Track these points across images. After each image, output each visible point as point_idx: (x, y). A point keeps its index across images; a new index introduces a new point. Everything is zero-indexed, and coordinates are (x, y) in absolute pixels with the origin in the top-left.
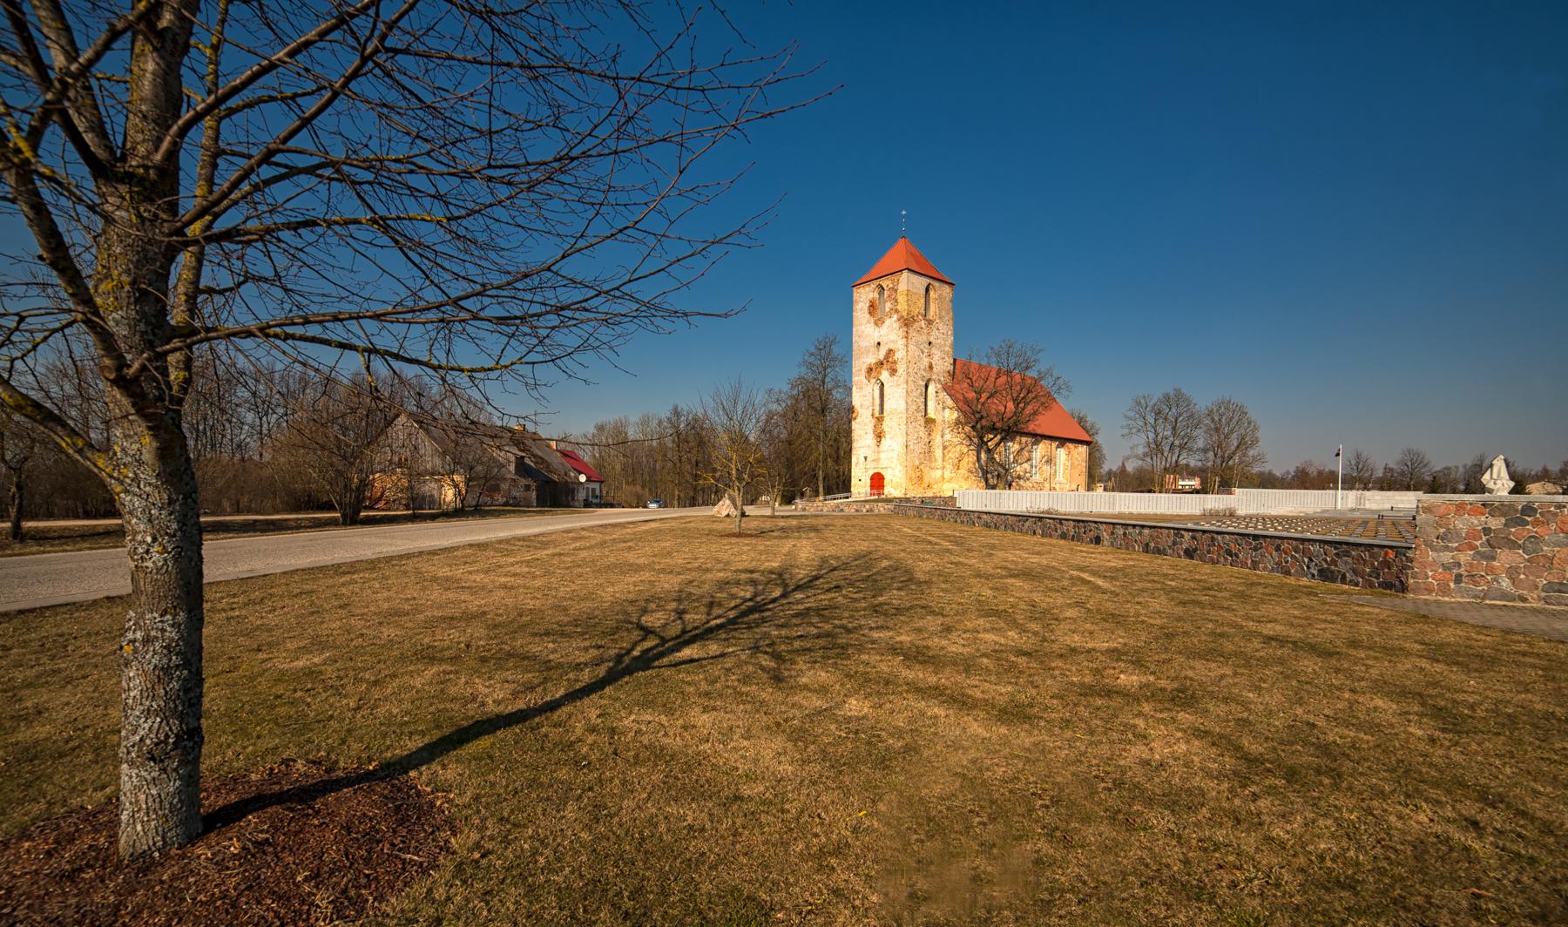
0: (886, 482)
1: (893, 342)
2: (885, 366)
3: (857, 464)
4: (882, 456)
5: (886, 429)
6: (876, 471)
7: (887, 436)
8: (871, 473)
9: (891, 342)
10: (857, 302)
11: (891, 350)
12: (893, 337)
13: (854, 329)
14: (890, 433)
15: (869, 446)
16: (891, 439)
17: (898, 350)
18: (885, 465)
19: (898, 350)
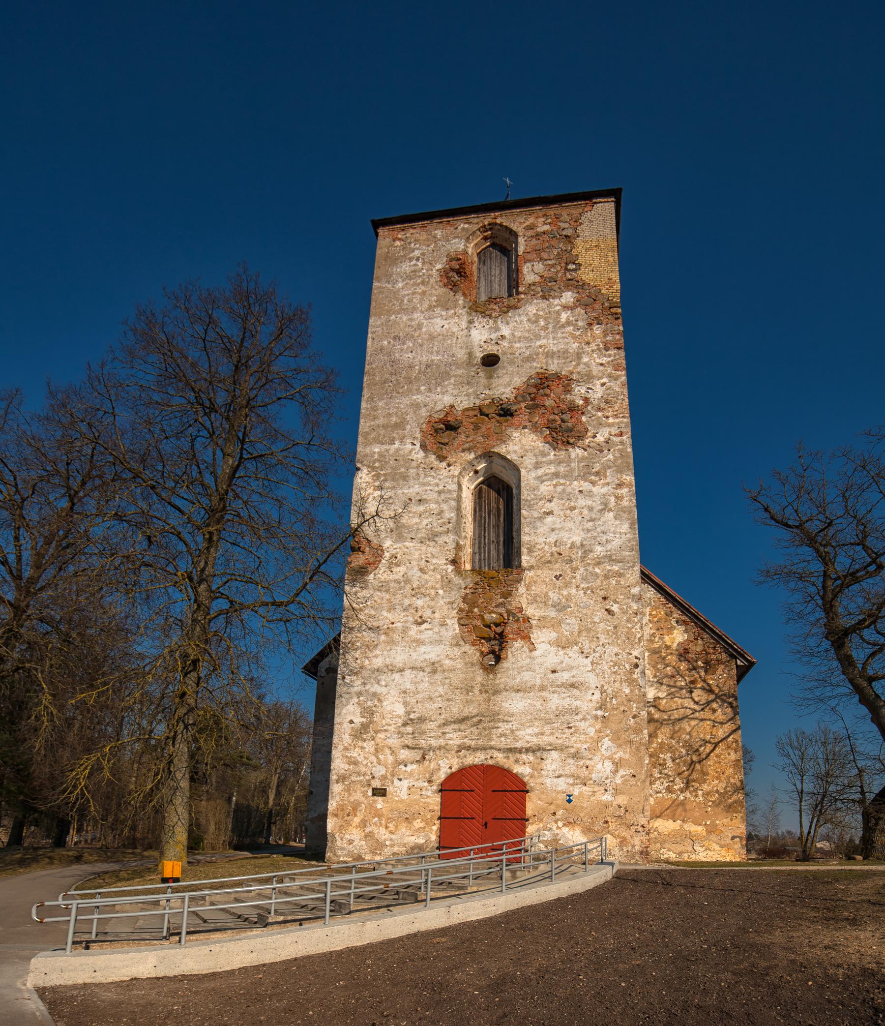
0: (531, 806)
1: (564, 354)
2: (523, 417)
3: (361, 733)
4: (515, 704)
5: (531, 611)
6: (477, 759)
7: (541, 637)
8: (446, 766)
9: (550, 355)
10: (394, 260)
11: (558, 377)
12: (550, 343)
13: (374, 322)
14: (556, 625)
15: (434, 668)
16: (563, 644)
17: (589, 377)
18: (527, 736)
19: (589, 377)
